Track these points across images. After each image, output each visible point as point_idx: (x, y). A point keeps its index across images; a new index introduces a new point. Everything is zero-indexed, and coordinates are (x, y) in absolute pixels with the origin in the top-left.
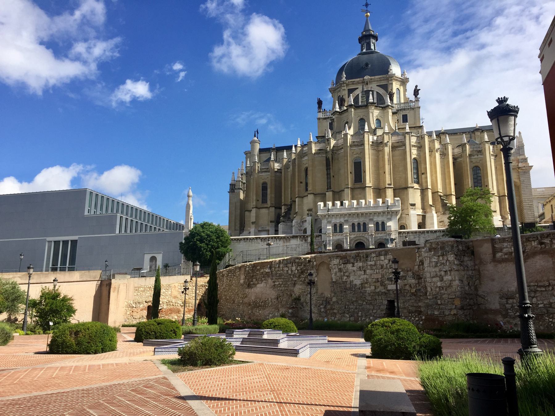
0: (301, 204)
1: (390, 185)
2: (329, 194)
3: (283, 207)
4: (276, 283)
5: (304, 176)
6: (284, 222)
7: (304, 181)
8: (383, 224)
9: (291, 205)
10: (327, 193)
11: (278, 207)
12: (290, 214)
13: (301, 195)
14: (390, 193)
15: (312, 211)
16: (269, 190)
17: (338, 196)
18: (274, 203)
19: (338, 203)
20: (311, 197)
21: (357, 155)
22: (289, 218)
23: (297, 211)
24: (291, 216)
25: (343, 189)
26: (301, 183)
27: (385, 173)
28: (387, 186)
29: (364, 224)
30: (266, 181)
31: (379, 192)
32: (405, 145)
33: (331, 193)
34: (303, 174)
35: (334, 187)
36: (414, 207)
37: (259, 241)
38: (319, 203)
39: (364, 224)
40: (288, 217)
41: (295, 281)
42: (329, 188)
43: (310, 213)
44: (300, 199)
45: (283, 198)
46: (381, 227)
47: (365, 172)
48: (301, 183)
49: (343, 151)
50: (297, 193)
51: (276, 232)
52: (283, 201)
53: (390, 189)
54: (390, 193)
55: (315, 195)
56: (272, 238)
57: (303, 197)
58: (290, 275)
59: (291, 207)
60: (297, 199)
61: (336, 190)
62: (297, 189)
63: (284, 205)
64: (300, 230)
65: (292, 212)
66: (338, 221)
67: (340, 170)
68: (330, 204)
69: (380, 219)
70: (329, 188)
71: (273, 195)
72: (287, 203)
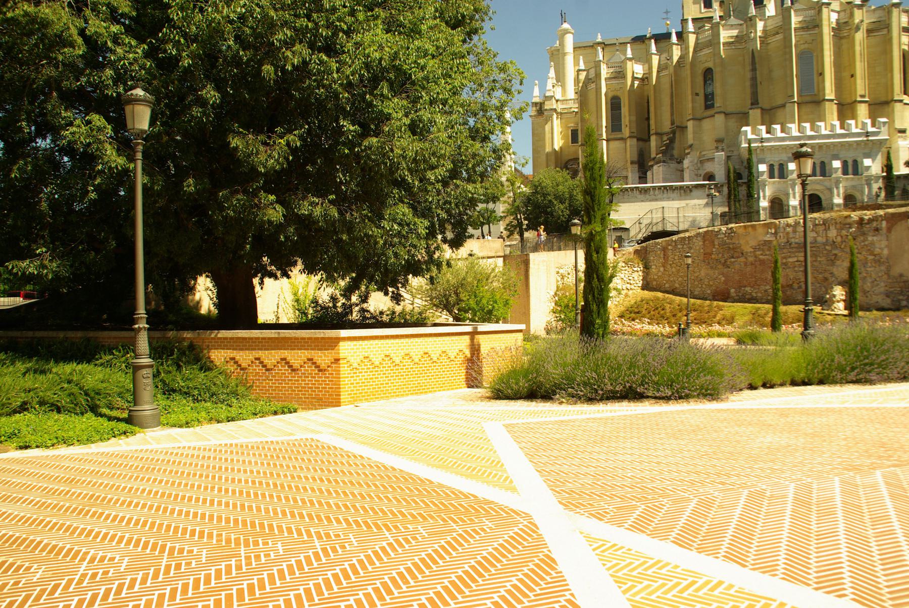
0: (698, 132)
1: (862, 96)
2: (755, 114)
3: (653, 138)
4: (790, 260)
5: (702, 83)
6: (664, 162)
7: (702, 91)
8: (855, 163)
9: (674, 132)
10: (751, 111)
11: (643, 137)
12: (673, 149)
13: (698, 116)
14: (862, 110)
15: (728, 142)
16: (625, 111)
17: (770, 116)
18: (634, 130)
19: (778, 127)
20: (720, 119)
21: (806, 46)
22: (672, 155)
23: (690, 142)
24: (676, 153)
25: (780, 102)
26: (697, 94)
27: (852, 76)
28: (859, 99)
29: (823, 163)
30: (619, 94)
31: (846, 110)
32: (888, 27)
33: (758, 111)
34: (700, 80)
35: (764, 102)
36: (903, 135)
37: (636, 193)
38: (744, 129)
39: (823, 163)
40: (672, 153)
41: (836, 255)
42: (755, 103)
43: (720, 146)
44: (696, 122)
45: (652, 122)
46: (853, 168)
47: (821, 74)
48: (697, 94)
49: (779, 37)
50: (690, 112)
51: (643, 178)
52: (653, 127)
53: (863, 105)
54: (862, 110)
55: (726, 114)
56: (660, 188)
57: (700, 120)
58: (825, 244)
59: (674, 137)
60: (690, 124)
61: (766, 106)
62: (690, 105)
63: (656, 134)
64: (697, 175)
65: (676, 144)
66: (776, 159)
67: (771, 71)
68: (763, 128)
69: (850, 156)
70: (755, 103)
71: (634, 118)
72: (659, 131)
